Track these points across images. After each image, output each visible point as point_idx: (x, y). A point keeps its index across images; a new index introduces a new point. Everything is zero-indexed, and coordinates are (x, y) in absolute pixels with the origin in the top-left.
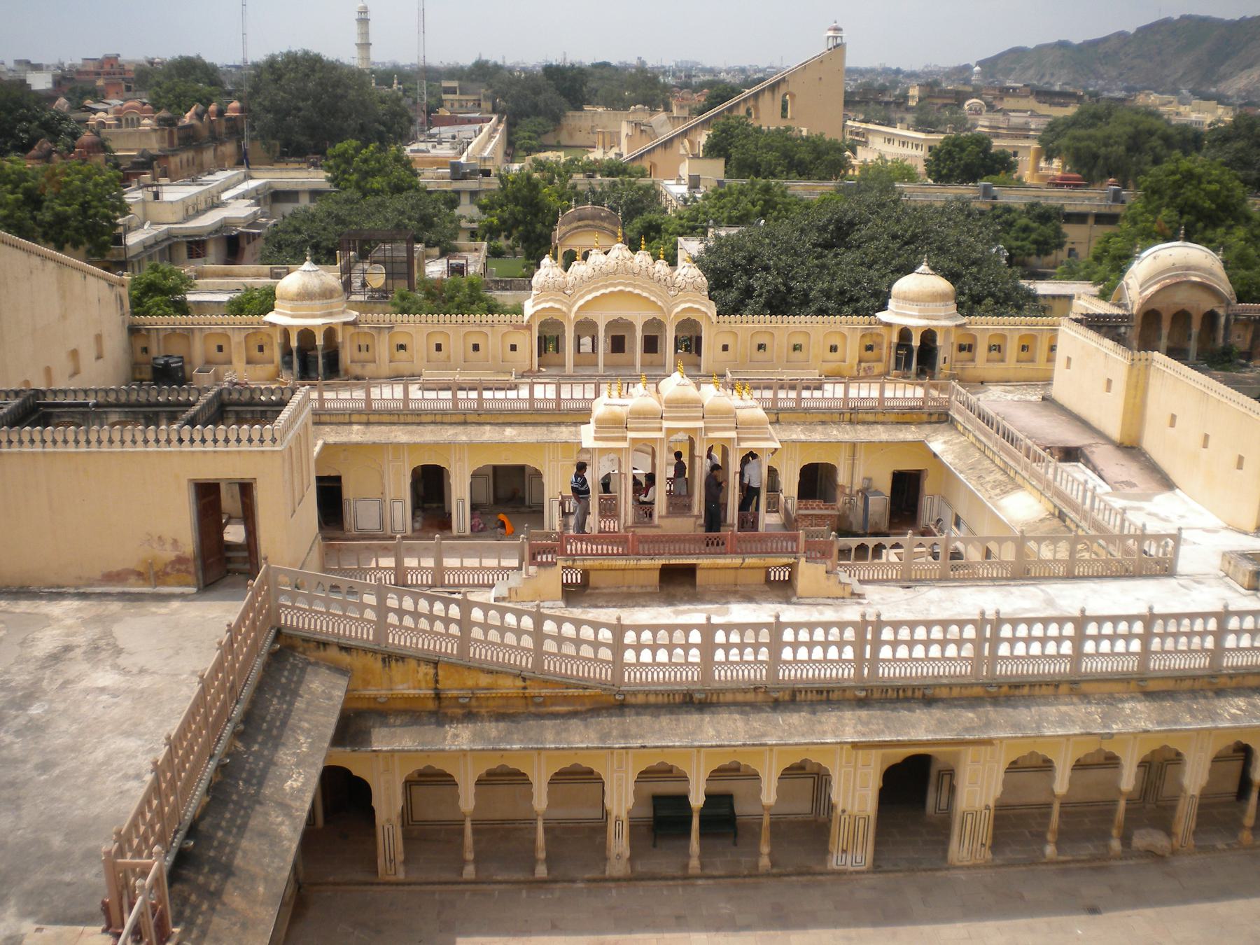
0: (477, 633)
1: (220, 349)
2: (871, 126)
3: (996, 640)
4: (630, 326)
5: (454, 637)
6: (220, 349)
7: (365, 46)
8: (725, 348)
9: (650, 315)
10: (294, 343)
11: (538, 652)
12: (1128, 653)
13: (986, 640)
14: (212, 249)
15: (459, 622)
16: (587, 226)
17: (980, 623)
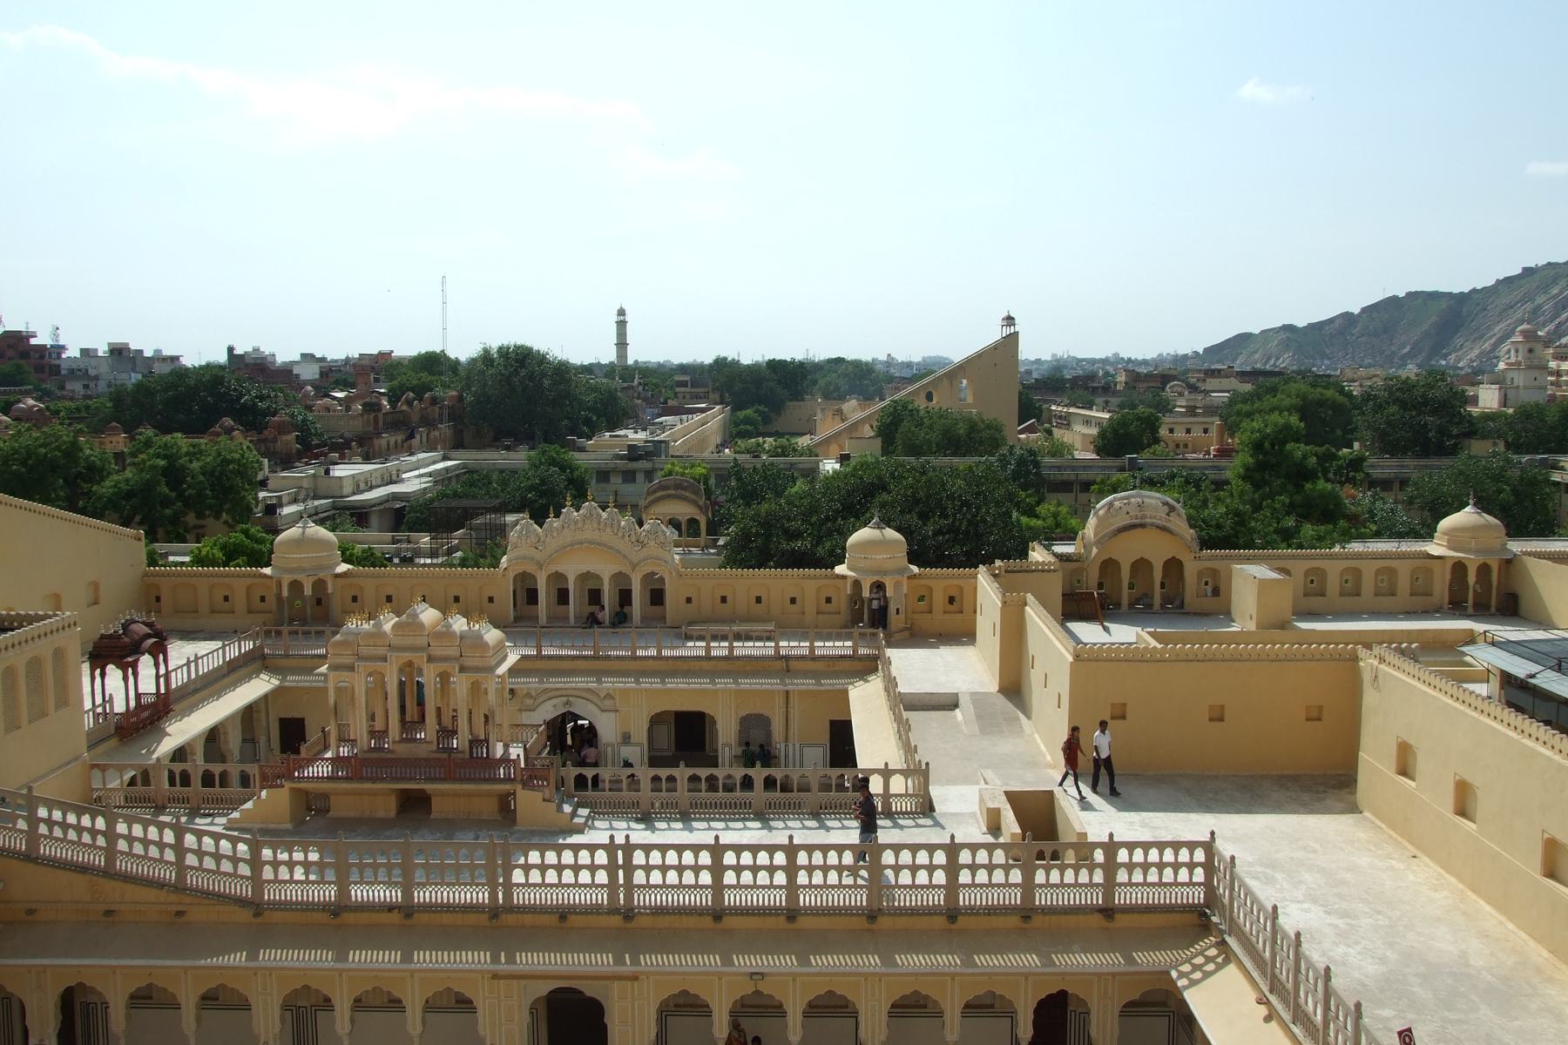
0: (122, 845)
1: (226, 599)
2: (1072, 410)
3: (629, 868)
4: (598, 578)
5: (101, 848)
6: (226, 599)
7: (622, 344)
8: (689, 600)
9: (616, 568)
10: (285, 593)
11: (180, 864)
12: (771, 886)
13: (619, 867)
14: (374, 520)
15: (104, 834)
16: (669, 496)
17: (611, 848)
